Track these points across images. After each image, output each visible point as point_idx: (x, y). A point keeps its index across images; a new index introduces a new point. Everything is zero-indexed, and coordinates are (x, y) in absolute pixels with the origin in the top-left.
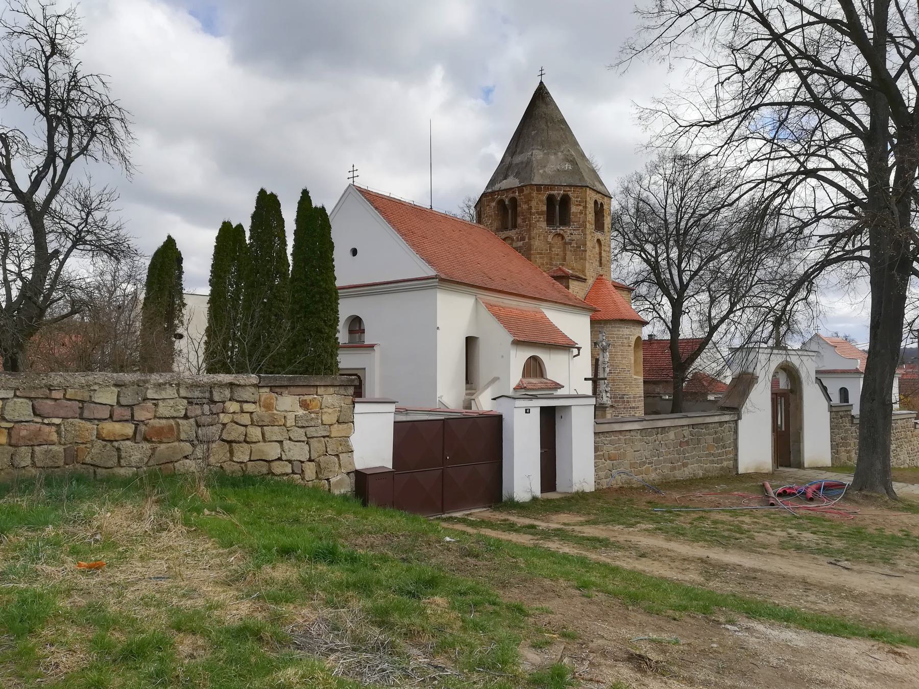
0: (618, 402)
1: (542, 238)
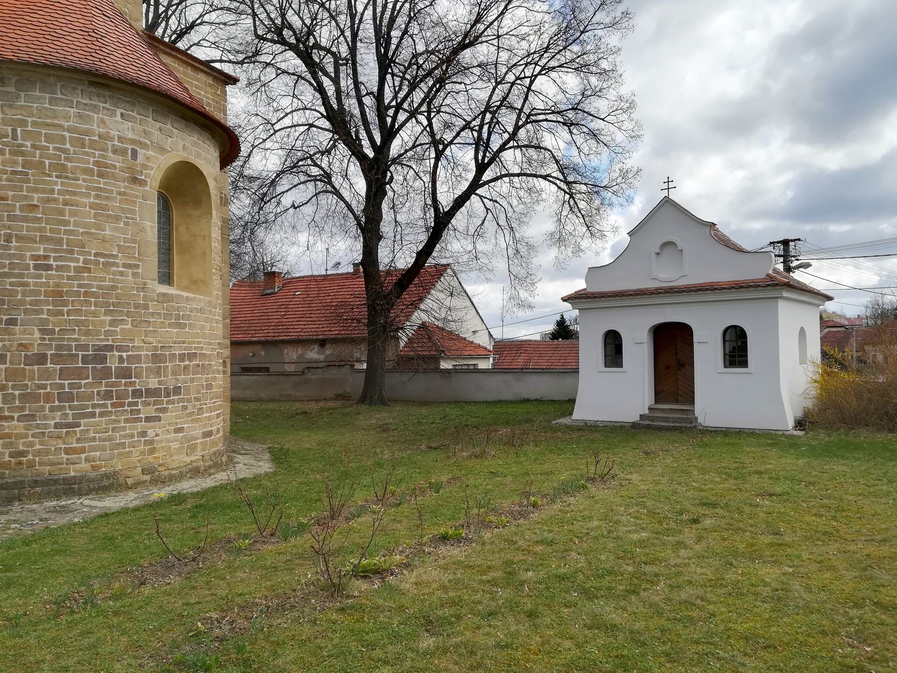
0: (79, 374)
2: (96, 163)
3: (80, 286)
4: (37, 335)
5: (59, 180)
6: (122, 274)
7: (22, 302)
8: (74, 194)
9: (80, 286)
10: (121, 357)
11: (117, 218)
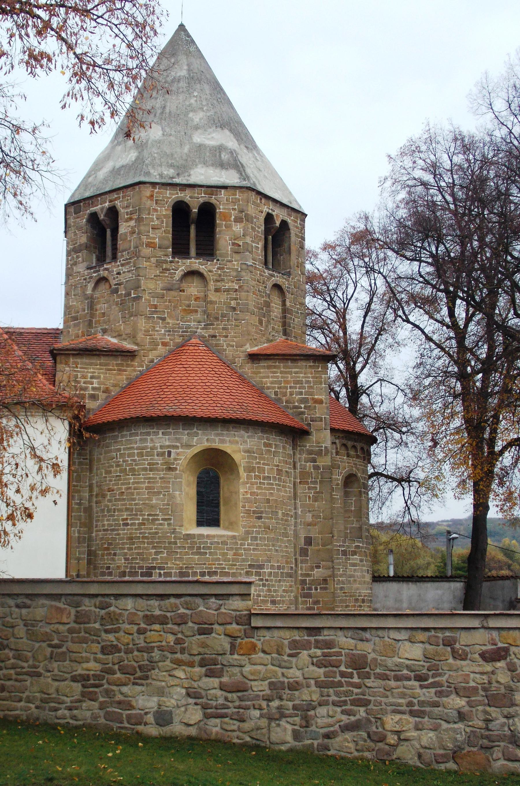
1: (79, 290)
2: (149, 464)
3: (140, 533)
4: (123, 561)
5: (132, 477)
6: (161, 524)
7: (118, 544)
8: (138, 483)
9: (140, 533)
10: (160, 573)
11: (159, 493)
